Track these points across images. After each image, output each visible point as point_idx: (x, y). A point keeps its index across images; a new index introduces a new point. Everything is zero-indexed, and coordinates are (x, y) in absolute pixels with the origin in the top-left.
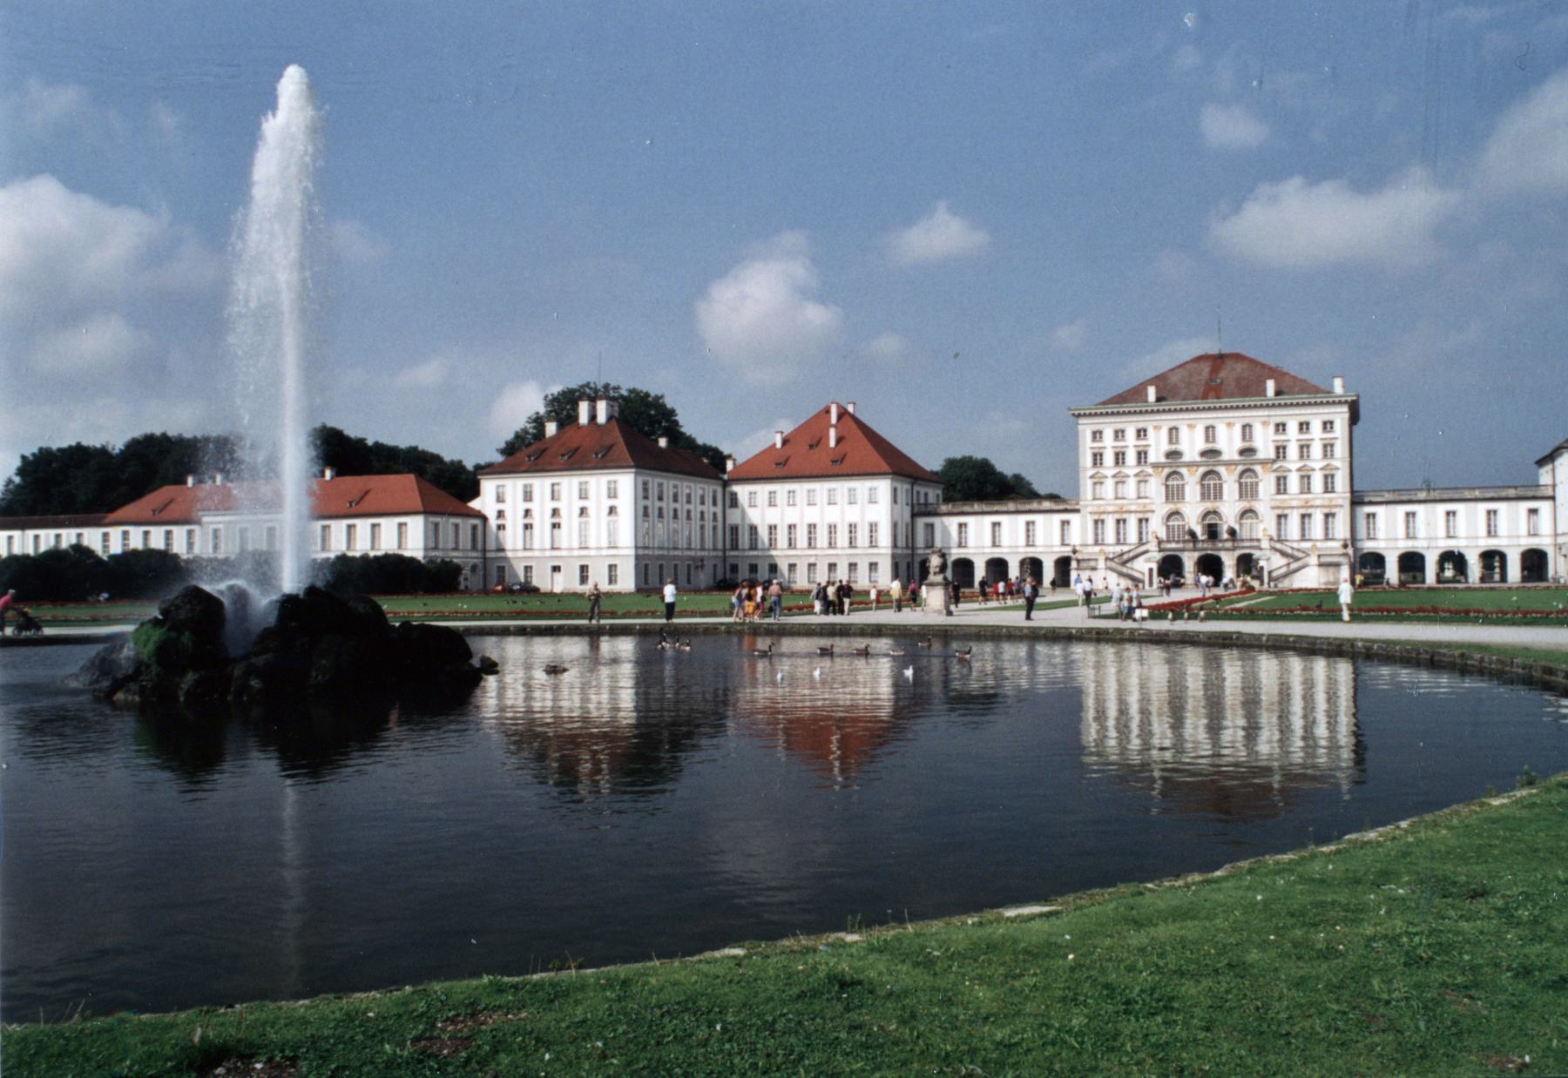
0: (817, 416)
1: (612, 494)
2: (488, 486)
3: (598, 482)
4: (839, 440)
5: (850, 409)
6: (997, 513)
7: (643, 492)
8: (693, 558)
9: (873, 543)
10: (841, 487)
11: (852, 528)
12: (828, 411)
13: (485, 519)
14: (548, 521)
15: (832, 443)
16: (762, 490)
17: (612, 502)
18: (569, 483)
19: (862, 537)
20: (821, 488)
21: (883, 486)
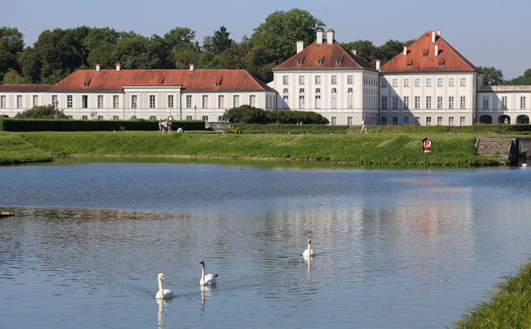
0: (423, 37)
1: (350, 81)
2: (278, 76)
3: (342, 76)
4: (440, 52)
5: (439, 33)
6: (523, 92)
7: (365, 82)
8: (373, 114)
9: (462, 107)
10: (445, 78)
11: (451, 99)
12: (429, 35)
13: (277, 93)
14: (314, 95)
15: (436, 54)
16: (400, 78)
17: (350, 86)
18: (326, 76)
19: (457, 103)
20: (434, 78)
21: (469, 78)
